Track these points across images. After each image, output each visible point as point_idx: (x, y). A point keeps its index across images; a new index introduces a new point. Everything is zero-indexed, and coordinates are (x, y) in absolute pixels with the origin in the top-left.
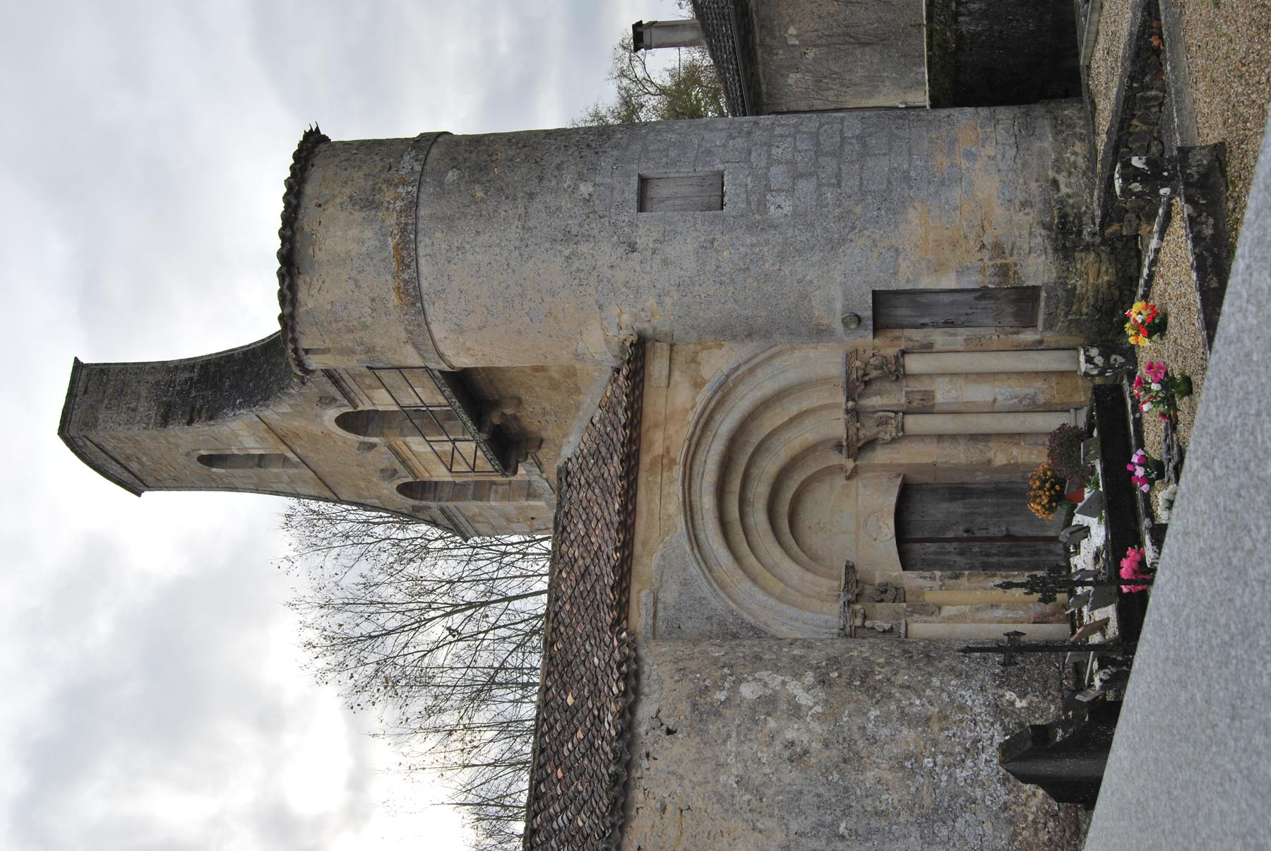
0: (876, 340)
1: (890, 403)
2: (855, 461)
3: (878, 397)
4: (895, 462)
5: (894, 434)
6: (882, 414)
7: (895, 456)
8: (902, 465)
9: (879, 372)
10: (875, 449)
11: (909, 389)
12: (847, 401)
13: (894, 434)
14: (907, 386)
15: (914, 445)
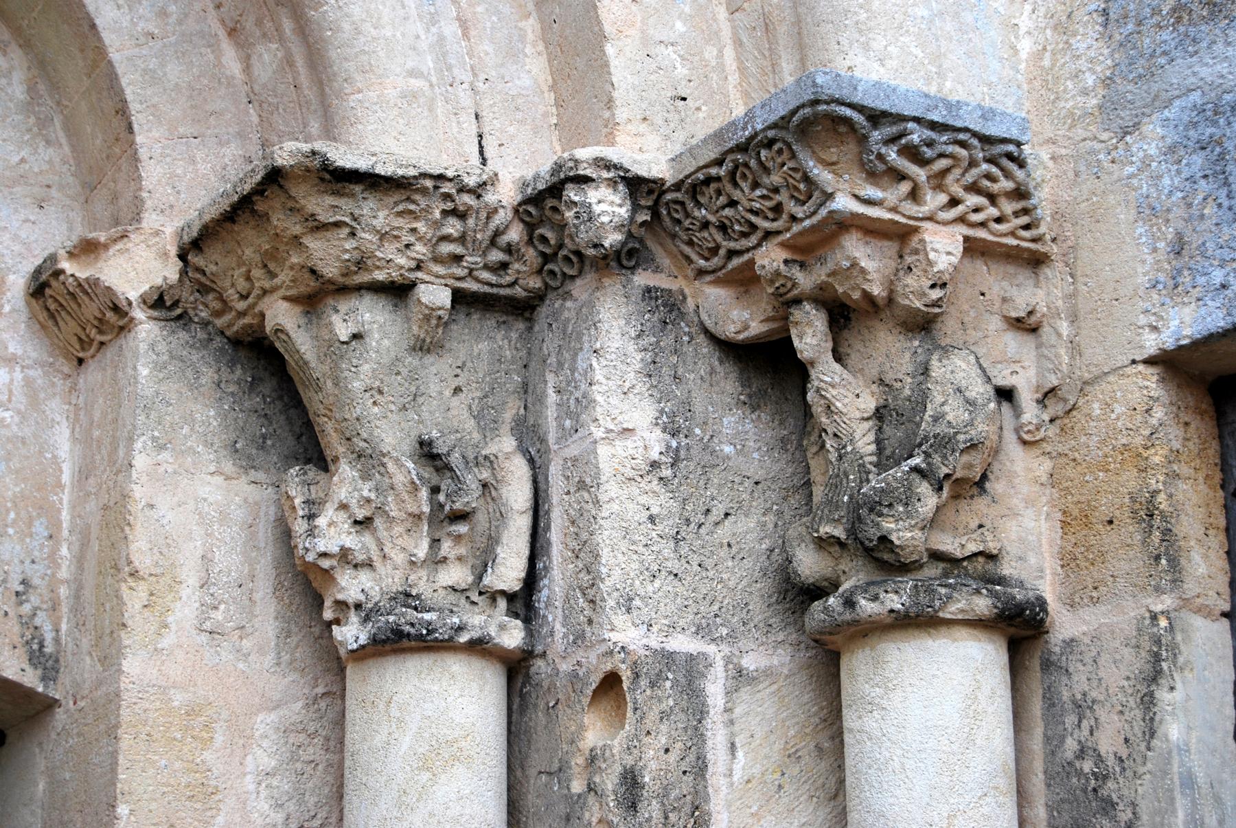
0: (1150, 382)
1: (607, 539)
2: (159, 302)
3: (655, 443)
4: (134, 598)
5: (351, 586)
6: (518, 494)
7: (185, 610)
8: (110, 659)
9: (864, 442)
10: (249, 465)
11: (715, 689)
12: (635, 185)
13: (351, 586)
14: (739, 677)
15: (263, 757)
